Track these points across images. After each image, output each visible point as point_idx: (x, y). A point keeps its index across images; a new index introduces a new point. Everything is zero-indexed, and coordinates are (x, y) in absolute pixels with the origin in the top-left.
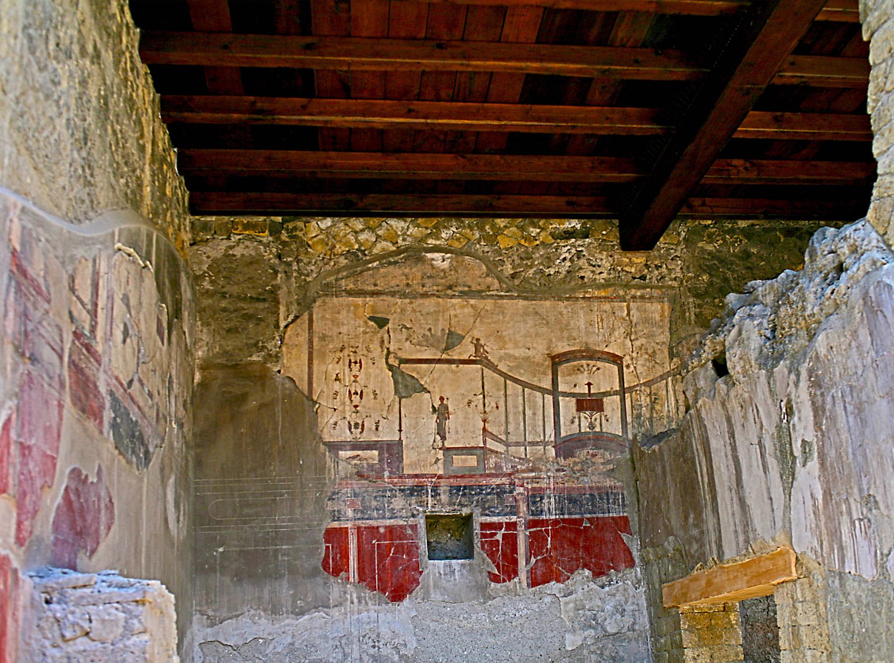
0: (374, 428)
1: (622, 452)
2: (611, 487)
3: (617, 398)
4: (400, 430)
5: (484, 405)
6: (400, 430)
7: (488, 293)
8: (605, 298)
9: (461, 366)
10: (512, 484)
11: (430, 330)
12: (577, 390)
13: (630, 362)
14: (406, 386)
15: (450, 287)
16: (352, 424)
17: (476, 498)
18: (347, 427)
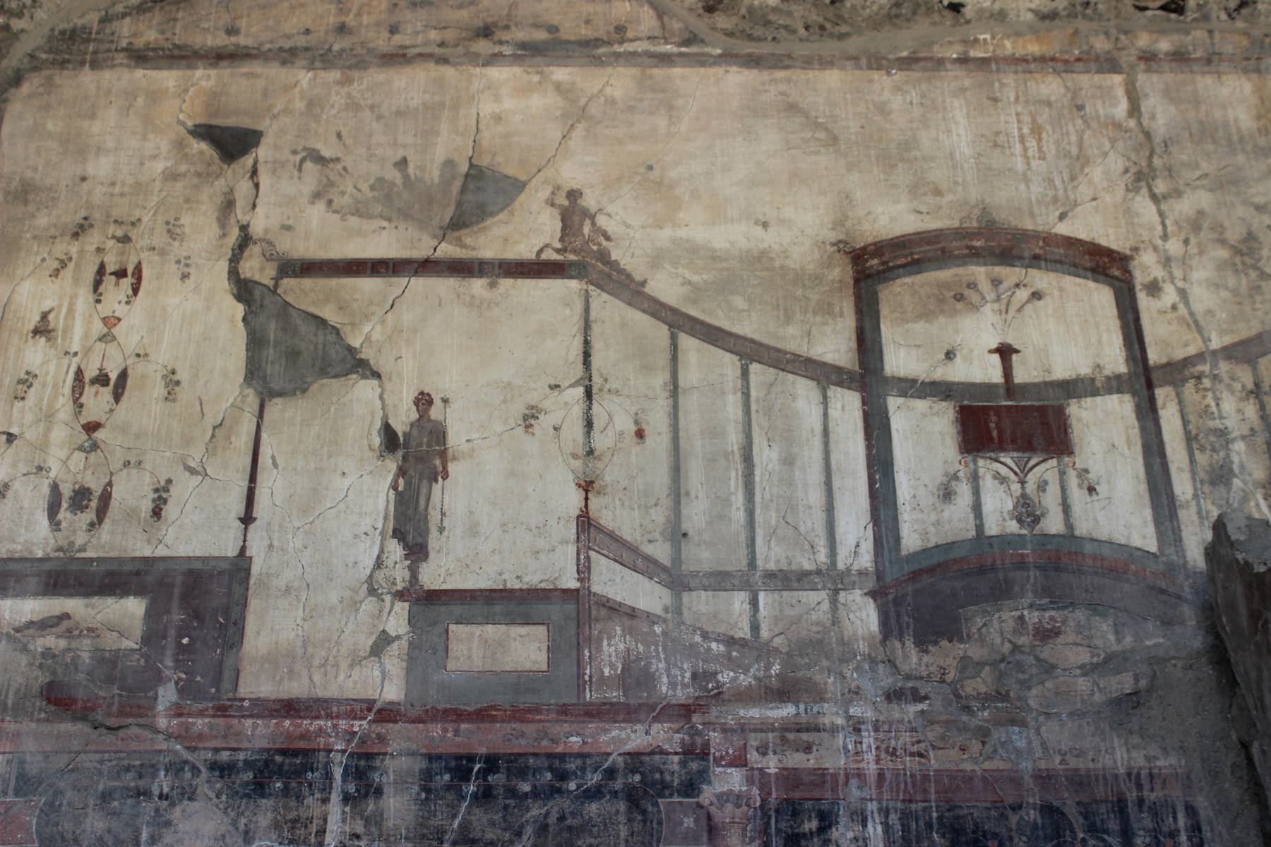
0: (146, 506)
1: (1167, 623)
2: (1134, 777)
3: (1121, 407)
4: (247, 519)
5: (589, 425)
6: (247, 519)
7: (618, 48)
8: (1042, 60)
9: (506, 283)
10: (696, 752)
11: (402, 163)
12: (959, 372)
13: (1158, 272)
14: (293, 355)
15: (486, 32)
17: (536, 811)
18: (43, 505)
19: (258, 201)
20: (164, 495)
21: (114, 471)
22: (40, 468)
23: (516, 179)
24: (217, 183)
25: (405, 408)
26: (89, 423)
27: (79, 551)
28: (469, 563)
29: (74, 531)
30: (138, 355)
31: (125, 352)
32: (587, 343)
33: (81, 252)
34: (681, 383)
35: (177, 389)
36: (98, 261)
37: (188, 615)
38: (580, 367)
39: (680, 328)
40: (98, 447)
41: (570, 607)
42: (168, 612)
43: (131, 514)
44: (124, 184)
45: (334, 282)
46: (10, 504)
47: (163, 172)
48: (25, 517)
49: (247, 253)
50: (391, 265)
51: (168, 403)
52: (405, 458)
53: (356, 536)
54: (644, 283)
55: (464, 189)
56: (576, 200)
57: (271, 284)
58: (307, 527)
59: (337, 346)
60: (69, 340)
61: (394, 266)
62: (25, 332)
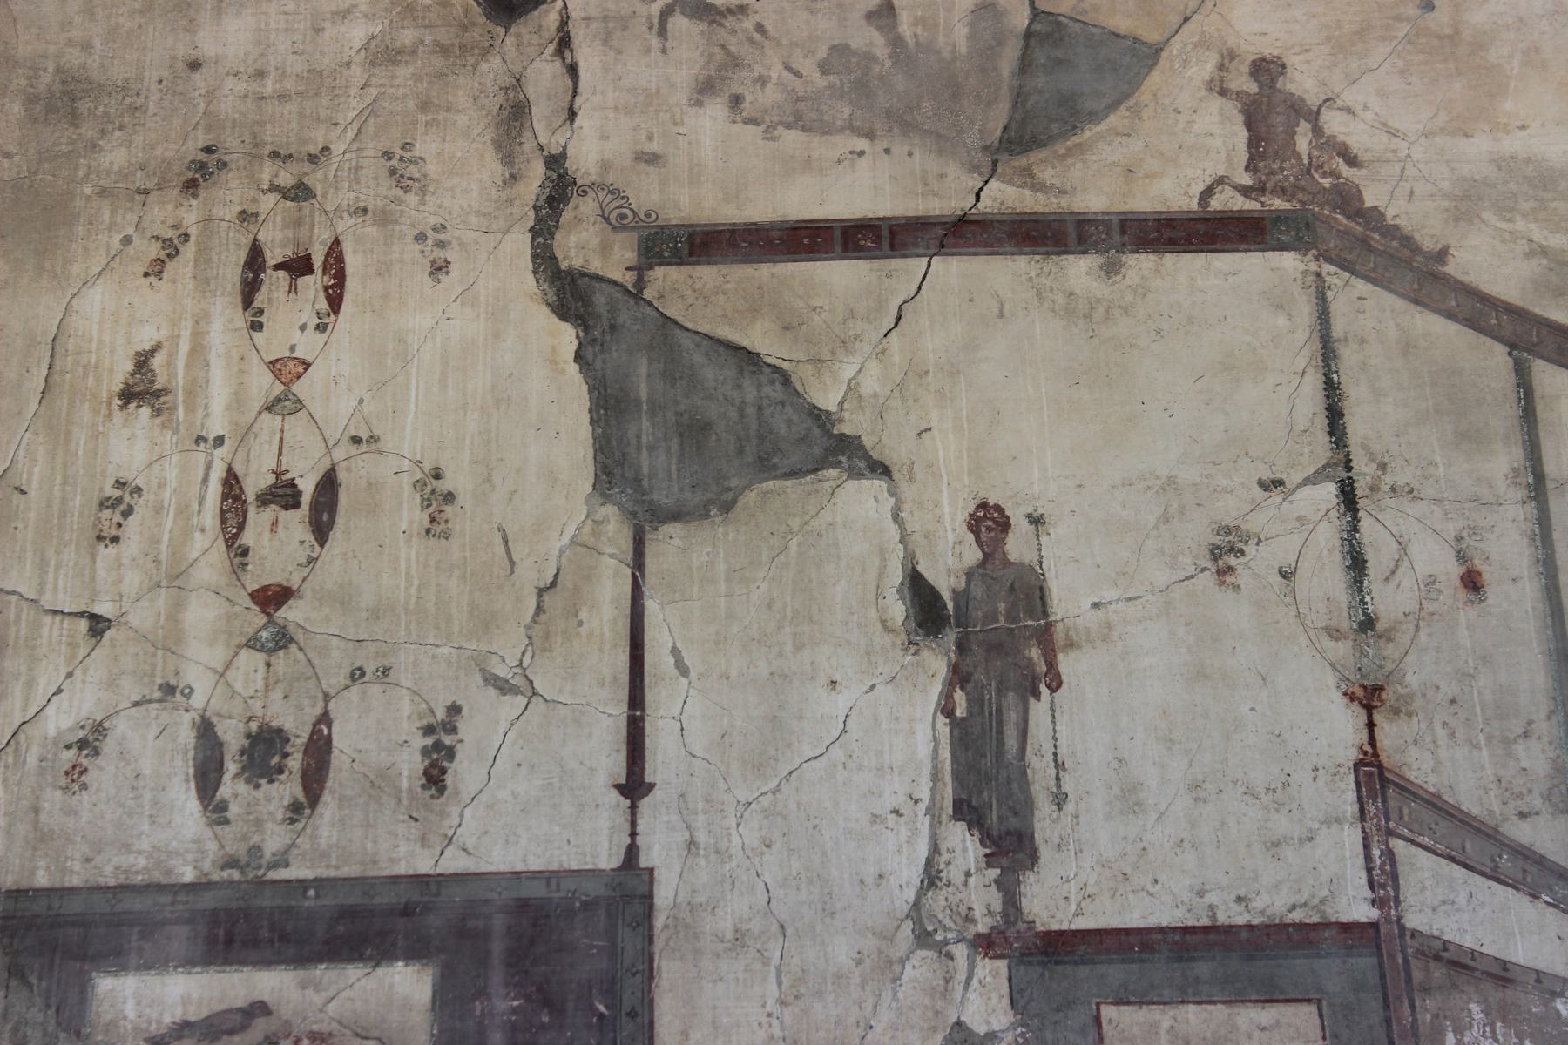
0: (410, 764)
4: (634, 787)
5: (1357, 564)
6: (634, 787)
9: (1140, 265)
14: (694, 432)
16: (232, 735)
19: (578, 101)
20: (448, 740)
21: (332, 692)
22: (169, 690)
23: (1136, 40)
24: (484, 66)
25: (951, 537)
26: (265, 588)
27: (274, 866)
28: (1128, 870)
29: (259, 823)
30: (356, 440)
31: (327, 434)
32: (1331, 388)
33: (207, 221)
34: (1550, 468)
35: (448, 509)
36: (246, 241)
37: (528, 999)
38: (1323, 438)
39: (1535, 350)
40: (292, 640)
41: (1364, 963)
42: (482, 993)
43: (378, 783)
44: (284, 75)
45: (764, 272)
46: (112, 769)
47: (366, 47)
48: (147, 796)
49: (567, 215)
50: (885, 233)
51: (433, 541)
52: (962, 647)
53: (875, 818)
54: (1442, 255)
55: (1025, 65)
56: (1273, 80)
57: (629, 279)
58: (766, 801)
59: (788, 408)
60: (200, 413)
61: (892, 232)
62: (105, 395)
